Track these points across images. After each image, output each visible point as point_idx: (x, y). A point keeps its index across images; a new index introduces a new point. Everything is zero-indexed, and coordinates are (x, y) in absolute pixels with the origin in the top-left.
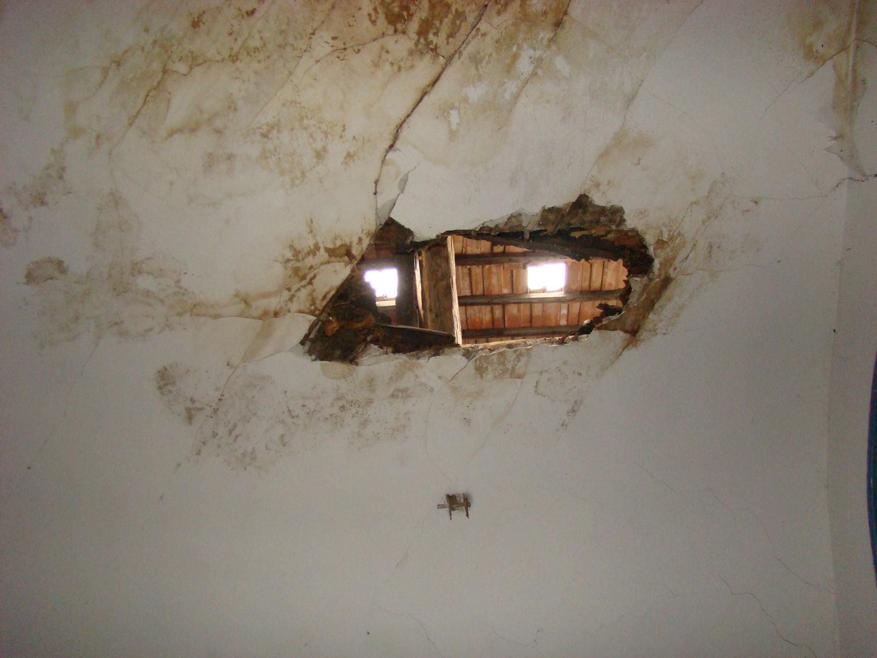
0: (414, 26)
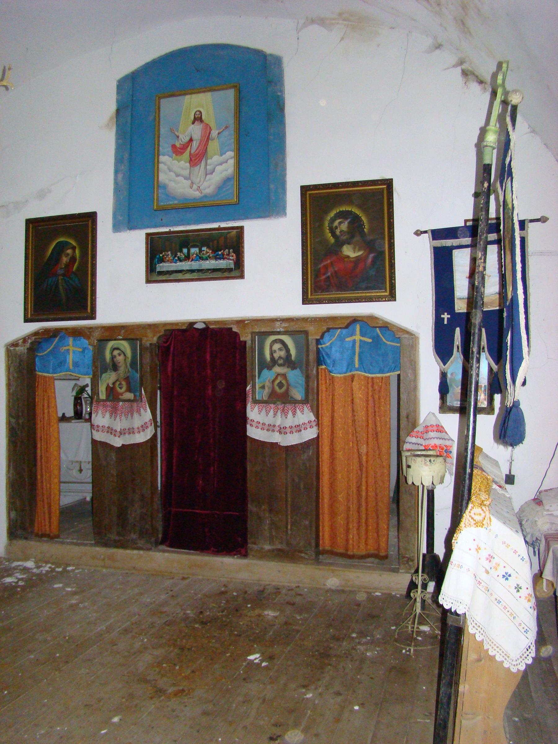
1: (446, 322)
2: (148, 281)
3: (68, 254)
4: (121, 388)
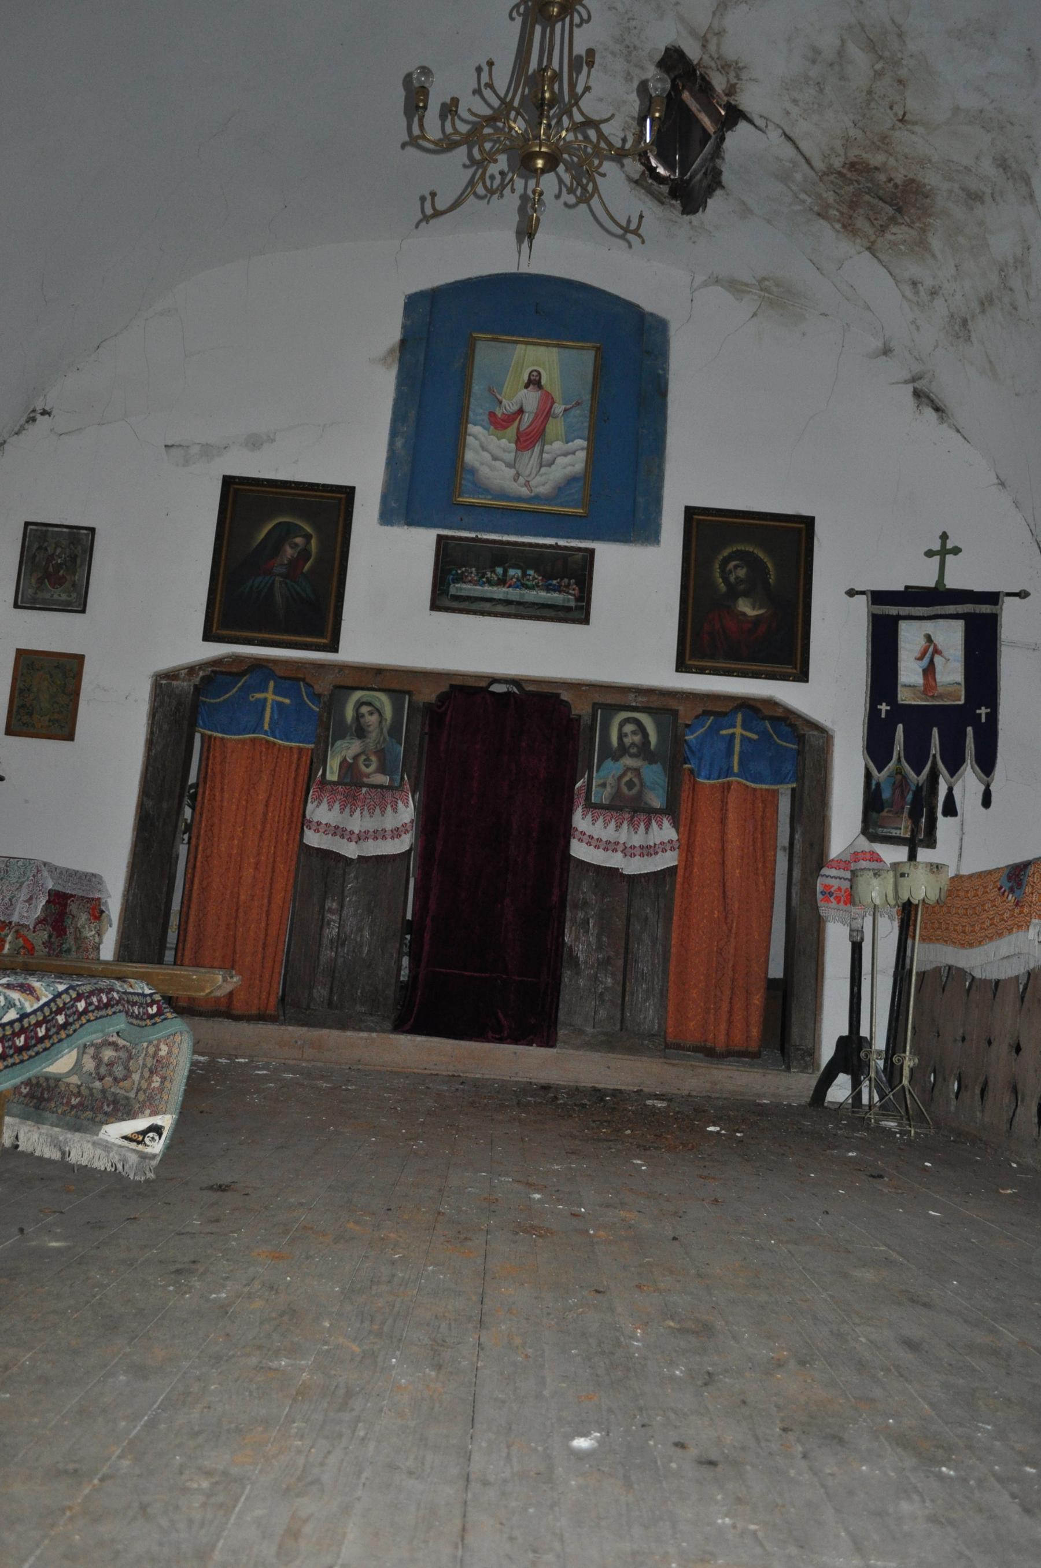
0: (845, 171)
1: (883, 716)
2: (434, 606)
3: (296, 545)
4: (367, 766)
